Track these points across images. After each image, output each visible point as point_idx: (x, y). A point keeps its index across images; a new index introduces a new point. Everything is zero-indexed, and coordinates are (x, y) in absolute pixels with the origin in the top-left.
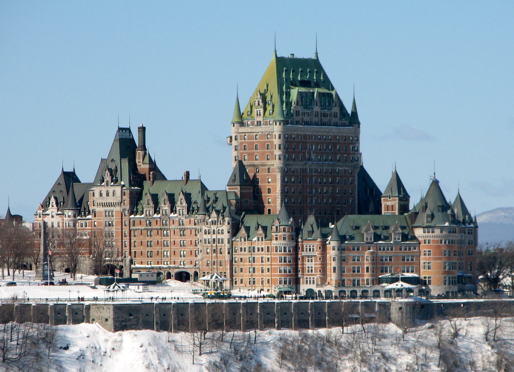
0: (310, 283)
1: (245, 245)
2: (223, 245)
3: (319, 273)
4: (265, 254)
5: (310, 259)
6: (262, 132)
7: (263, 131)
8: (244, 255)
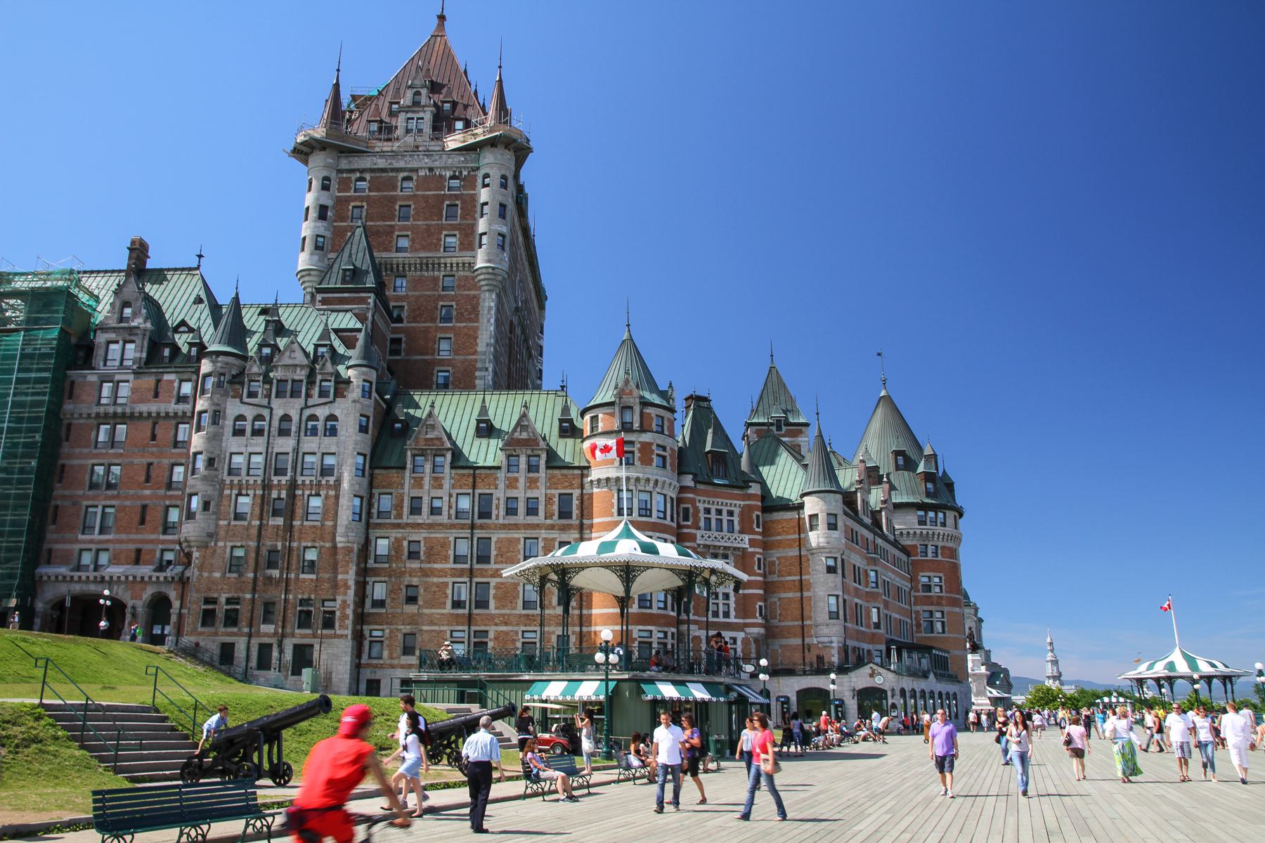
1: (440, 487)
2: (332, 480)
3: (760, 620)
4: (552, 527)
6: (431, 169)
7: (437, 164)
8: (431, 526)
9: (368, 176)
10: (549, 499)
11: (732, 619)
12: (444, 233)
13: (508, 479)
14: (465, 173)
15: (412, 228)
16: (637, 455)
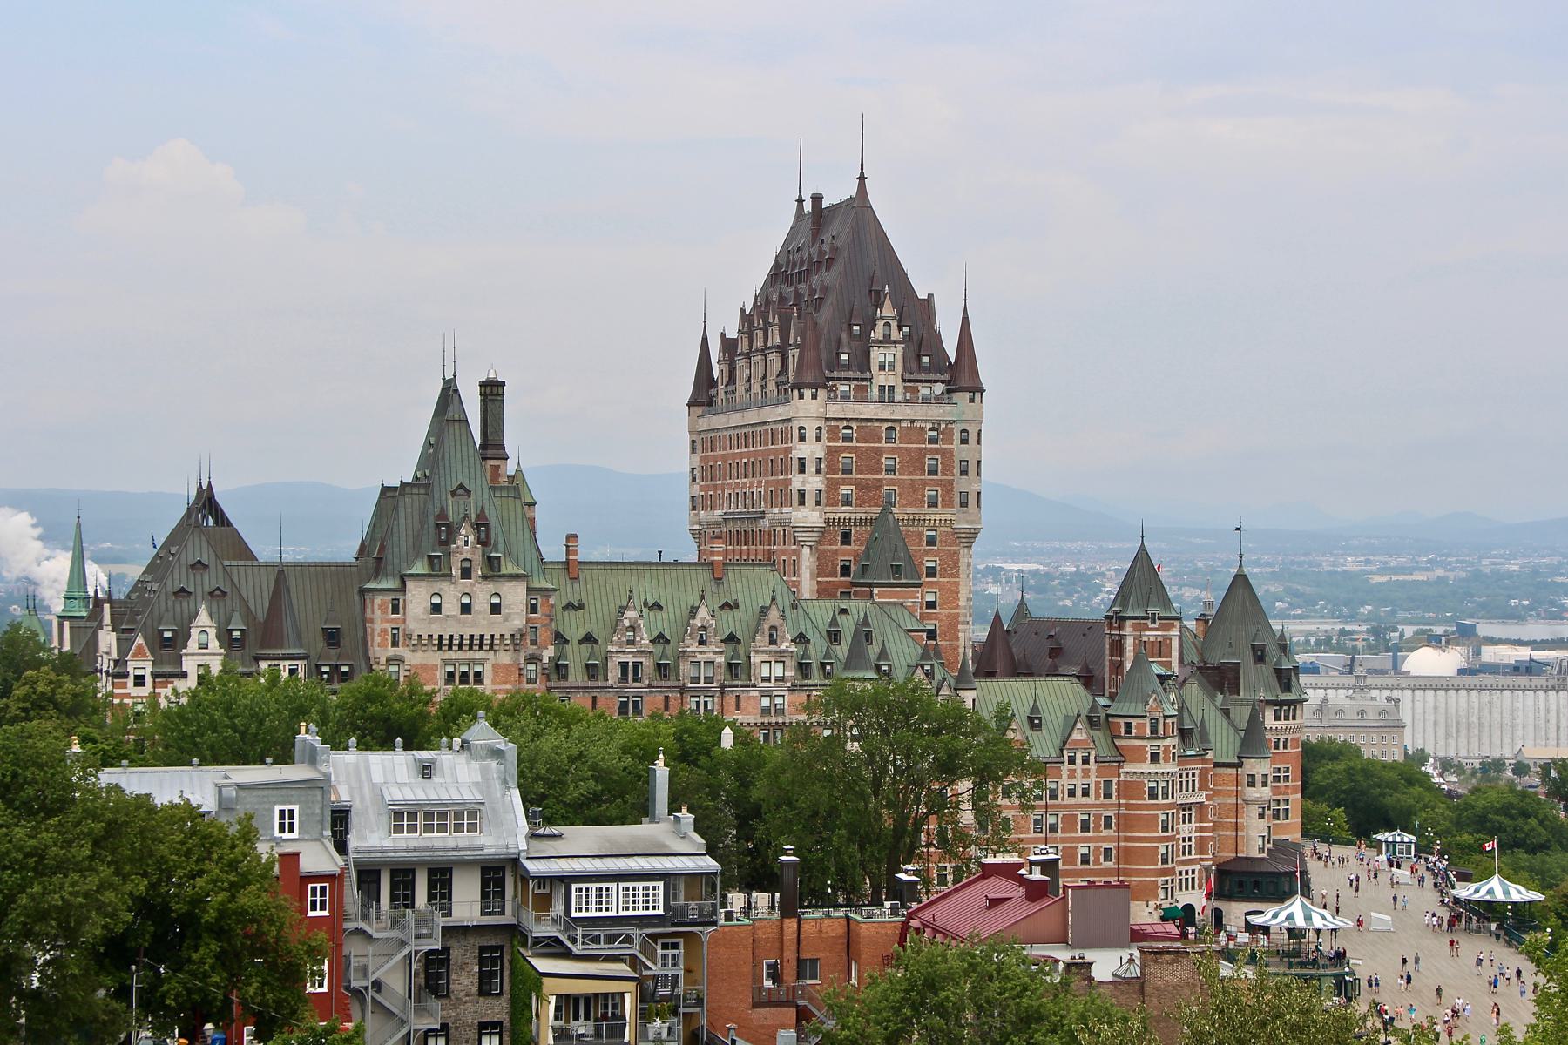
0: (1187, 888)
5: (1187, 813)
6: (912, 421)
9: (854, 426)
10: (1097, 783)
11: (1193, 856)
12: (927, 488)
13: (1069, 770)
14: (943, 426)
15: (899, 483)
16: (1162, 755)
